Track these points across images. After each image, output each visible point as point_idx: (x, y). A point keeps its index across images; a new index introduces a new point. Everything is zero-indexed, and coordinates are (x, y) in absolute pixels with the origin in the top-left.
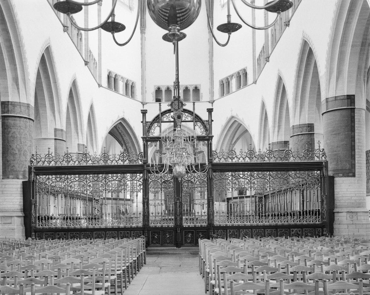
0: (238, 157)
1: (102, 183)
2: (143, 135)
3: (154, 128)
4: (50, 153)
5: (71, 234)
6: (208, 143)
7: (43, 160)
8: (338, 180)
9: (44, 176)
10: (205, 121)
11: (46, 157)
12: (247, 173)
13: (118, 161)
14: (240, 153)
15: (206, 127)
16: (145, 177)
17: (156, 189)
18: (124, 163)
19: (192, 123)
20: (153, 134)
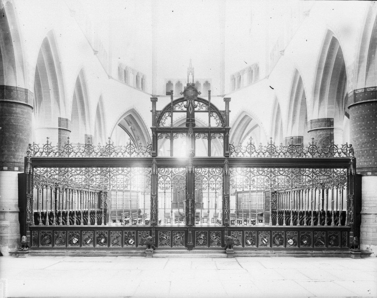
0: (258, 152)
2: (153, 126)
3: (164, 118)
4: (49, 144)
5: (70, 232)
6: (224, 135)
7: (41, 150)
8: (365, 179)
9: (42, 169)
10: (221, 111)
11: (45, 147)
13: (124, 154)
15: (222, 119)
16: (154, 171)
17: (166, 184)
18: (131, 155)
19: (207, 113)
20: (164, 125)
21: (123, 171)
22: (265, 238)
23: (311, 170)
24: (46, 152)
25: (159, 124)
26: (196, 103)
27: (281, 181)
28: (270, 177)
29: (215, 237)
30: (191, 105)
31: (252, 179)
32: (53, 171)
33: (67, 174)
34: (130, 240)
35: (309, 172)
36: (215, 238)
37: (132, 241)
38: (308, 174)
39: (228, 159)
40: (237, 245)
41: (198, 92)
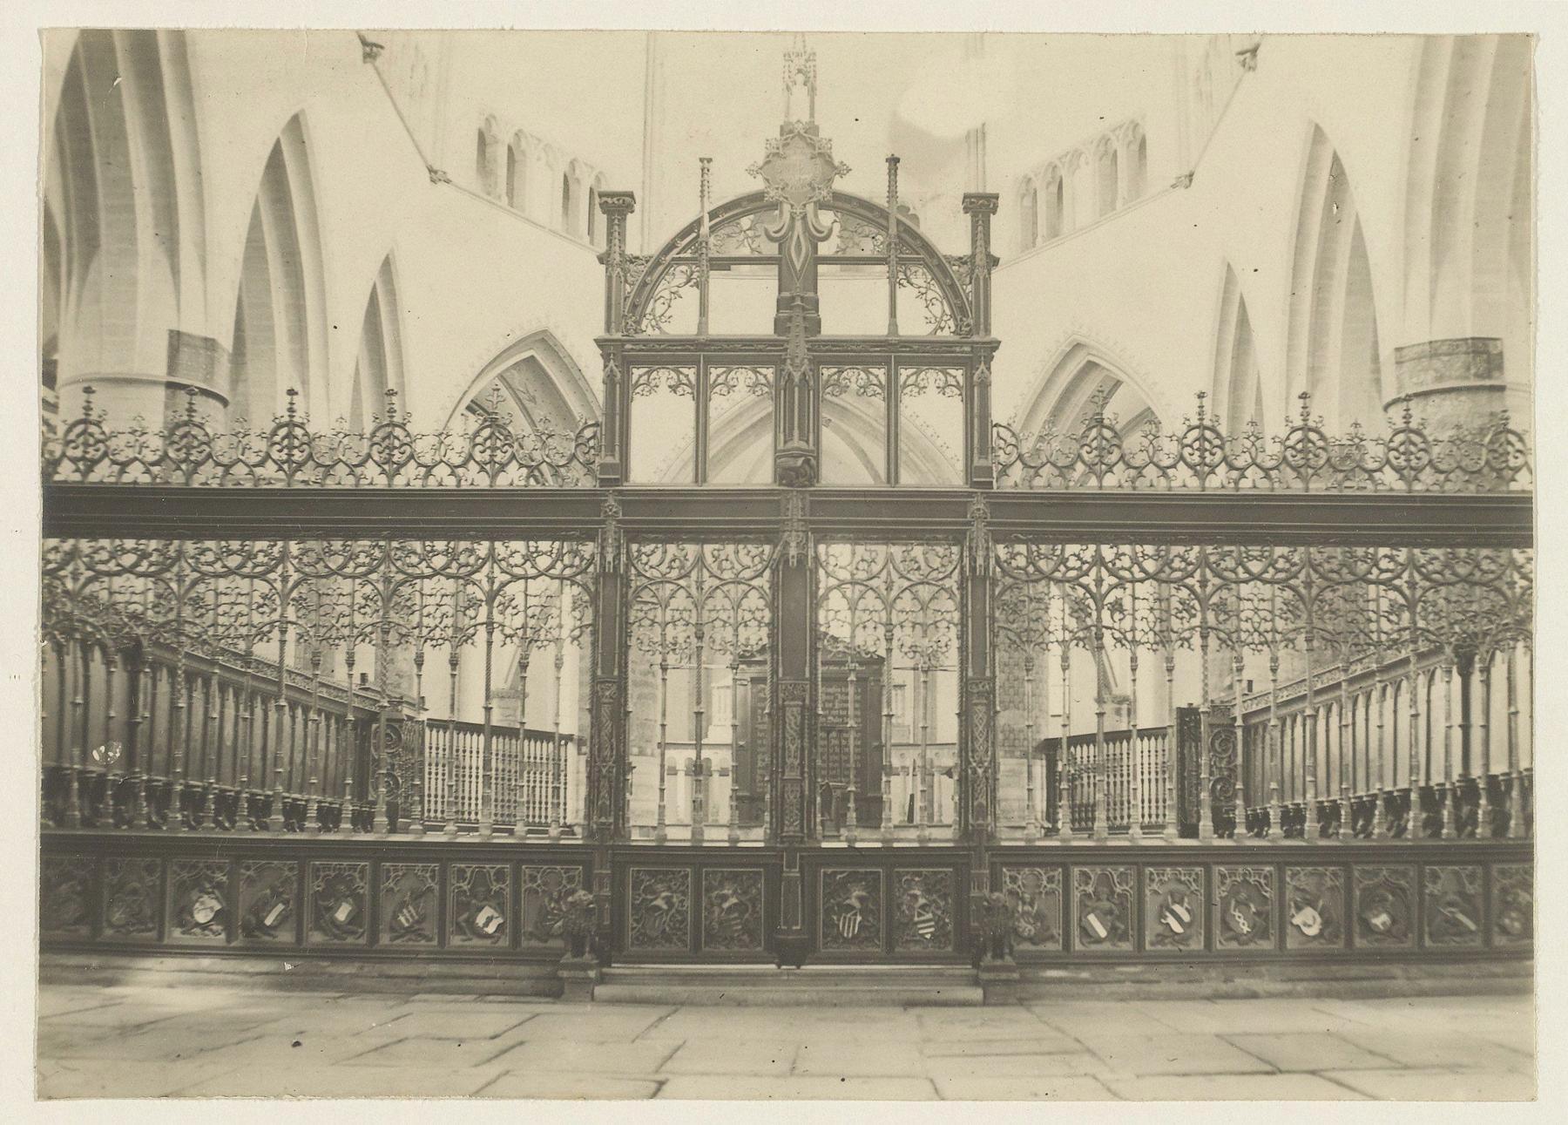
0: (1137, 462)
1: (368, 589)
2: (608, 329)
3: (666, 294)
4: (94, 417)
5: (183, 867)
6: (969, 377)
11: (72, 436)
12: (1180, 549)
14: (1146, 442)
15: (957, 295)
16: (610, 558)
18: (493, 477)
21: (453, 556)
22: (1181, 903)
23: (1402, 555)
24: (74, 460)
25: (638, 323)
26: (826, 218)
27: (1256, 610)
28: (1198, 590)
29: (922, 901)
30: (798, 224)
31: (1110, 598)
32: (210, 557)
33: (280, 569)
34: (480, 909)
35: (1391, 566)
36: (923, 907)
37: (489, 920)
38: (1389, 575)
39: (988, 496)
40: (1034, 944)
41: (836, 163)
